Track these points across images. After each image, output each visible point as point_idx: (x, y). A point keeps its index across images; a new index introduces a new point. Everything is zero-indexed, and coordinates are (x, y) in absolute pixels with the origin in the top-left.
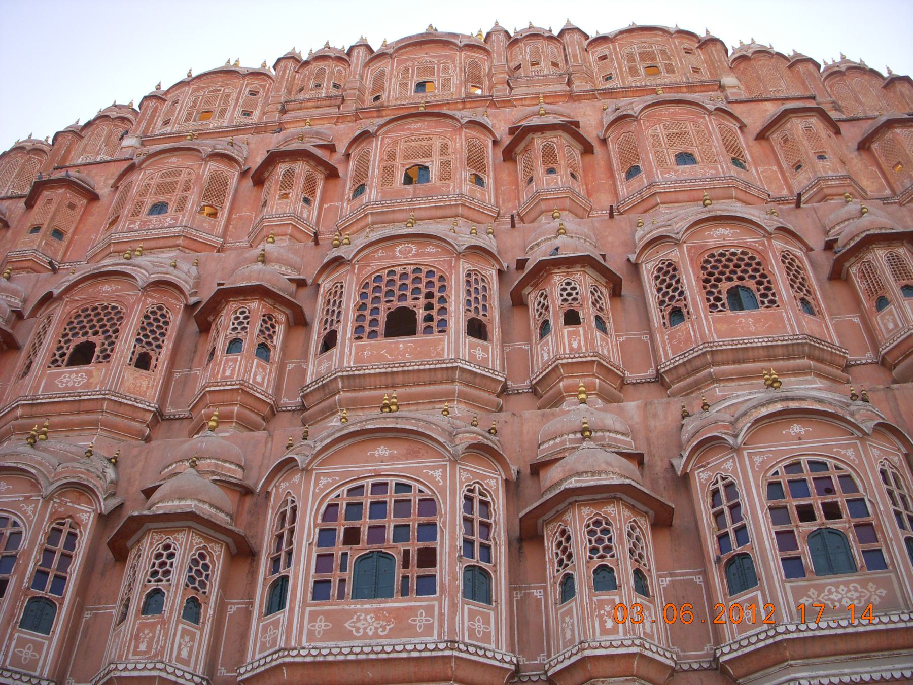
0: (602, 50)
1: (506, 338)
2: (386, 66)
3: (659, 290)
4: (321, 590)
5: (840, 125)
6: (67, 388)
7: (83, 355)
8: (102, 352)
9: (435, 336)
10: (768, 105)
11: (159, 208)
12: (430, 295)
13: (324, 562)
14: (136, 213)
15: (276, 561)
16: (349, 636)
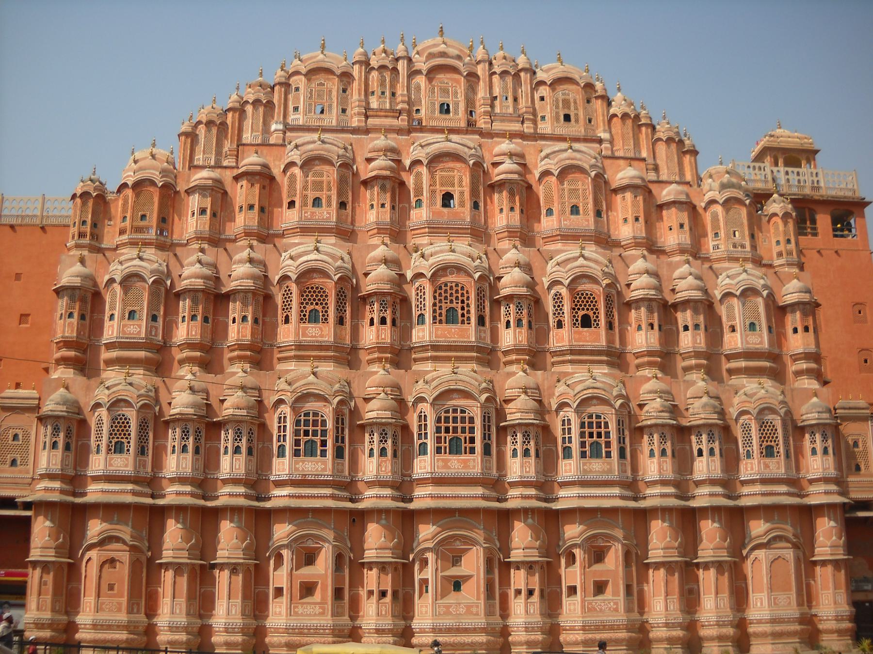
0: (544, 91)
1: (492, 320)
2: (421, 80)
3: (554, 306)
4: (438, 450)
5: (651, 186)
6: (312, 337)
7: (314, 317)
8: (323, 315)
9: (466, 326)
10: (622, 162)
11: (317, 202)
12: (463, 302)
13: (439, 440)
14: (306, 205)
15: (420, 435)
16: (450, 468)
